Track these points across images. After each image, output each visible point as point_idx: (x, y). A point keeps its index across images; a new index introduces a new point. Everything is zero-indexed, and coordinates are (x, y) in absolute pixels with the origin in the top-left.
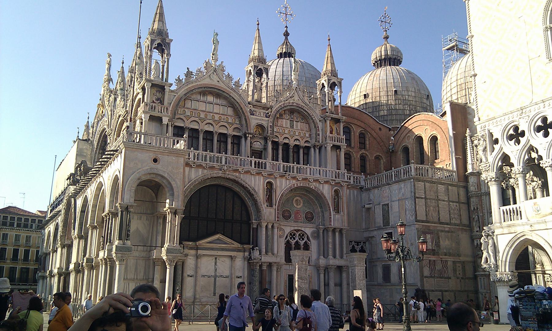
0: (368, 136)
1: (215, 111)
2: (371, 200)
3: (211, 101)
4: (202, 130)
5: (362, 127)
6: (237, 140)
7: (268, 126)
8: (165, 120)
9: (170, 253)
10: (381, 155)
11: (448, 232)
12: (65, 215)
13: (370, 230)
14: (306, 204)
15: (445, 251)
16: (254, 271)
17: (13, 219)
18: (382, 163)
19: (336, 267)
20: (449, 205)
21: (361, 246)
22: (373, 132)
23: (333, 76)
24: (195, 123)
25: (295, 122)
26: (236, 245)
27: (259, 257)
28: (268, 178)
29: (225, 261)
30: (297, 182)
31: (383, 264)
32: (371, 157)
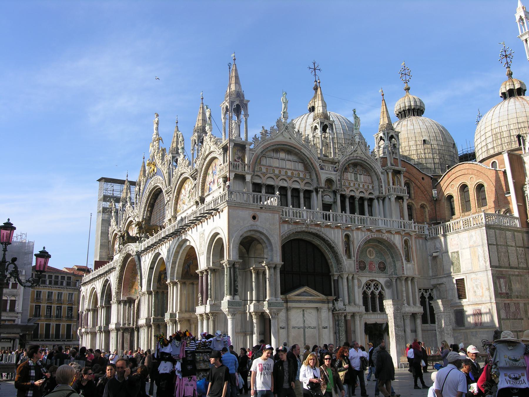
0: (412, 185)
1: (288, 167)
2: (437, 248)
4: (277, 186)
5: (407, 177)
6: (308, 194)
8: (248, 178)
10: (425, 203)
11: (518, 275)
12: (120, 272)
13: (438, 277)
14: (378, 255)
15: (517, 294)
16: (340, 322)
17: (57, 277)
18: (427, 211)
19: (411, 314)
20: (516, 250)
21: (429, 293)
23: (391, 129)
25: (358, 175)
26: (322, 297)
28: (346, 231)
29: (311, 312)
30: (371, 234)
31: (455, 309)
32: (417, 206)
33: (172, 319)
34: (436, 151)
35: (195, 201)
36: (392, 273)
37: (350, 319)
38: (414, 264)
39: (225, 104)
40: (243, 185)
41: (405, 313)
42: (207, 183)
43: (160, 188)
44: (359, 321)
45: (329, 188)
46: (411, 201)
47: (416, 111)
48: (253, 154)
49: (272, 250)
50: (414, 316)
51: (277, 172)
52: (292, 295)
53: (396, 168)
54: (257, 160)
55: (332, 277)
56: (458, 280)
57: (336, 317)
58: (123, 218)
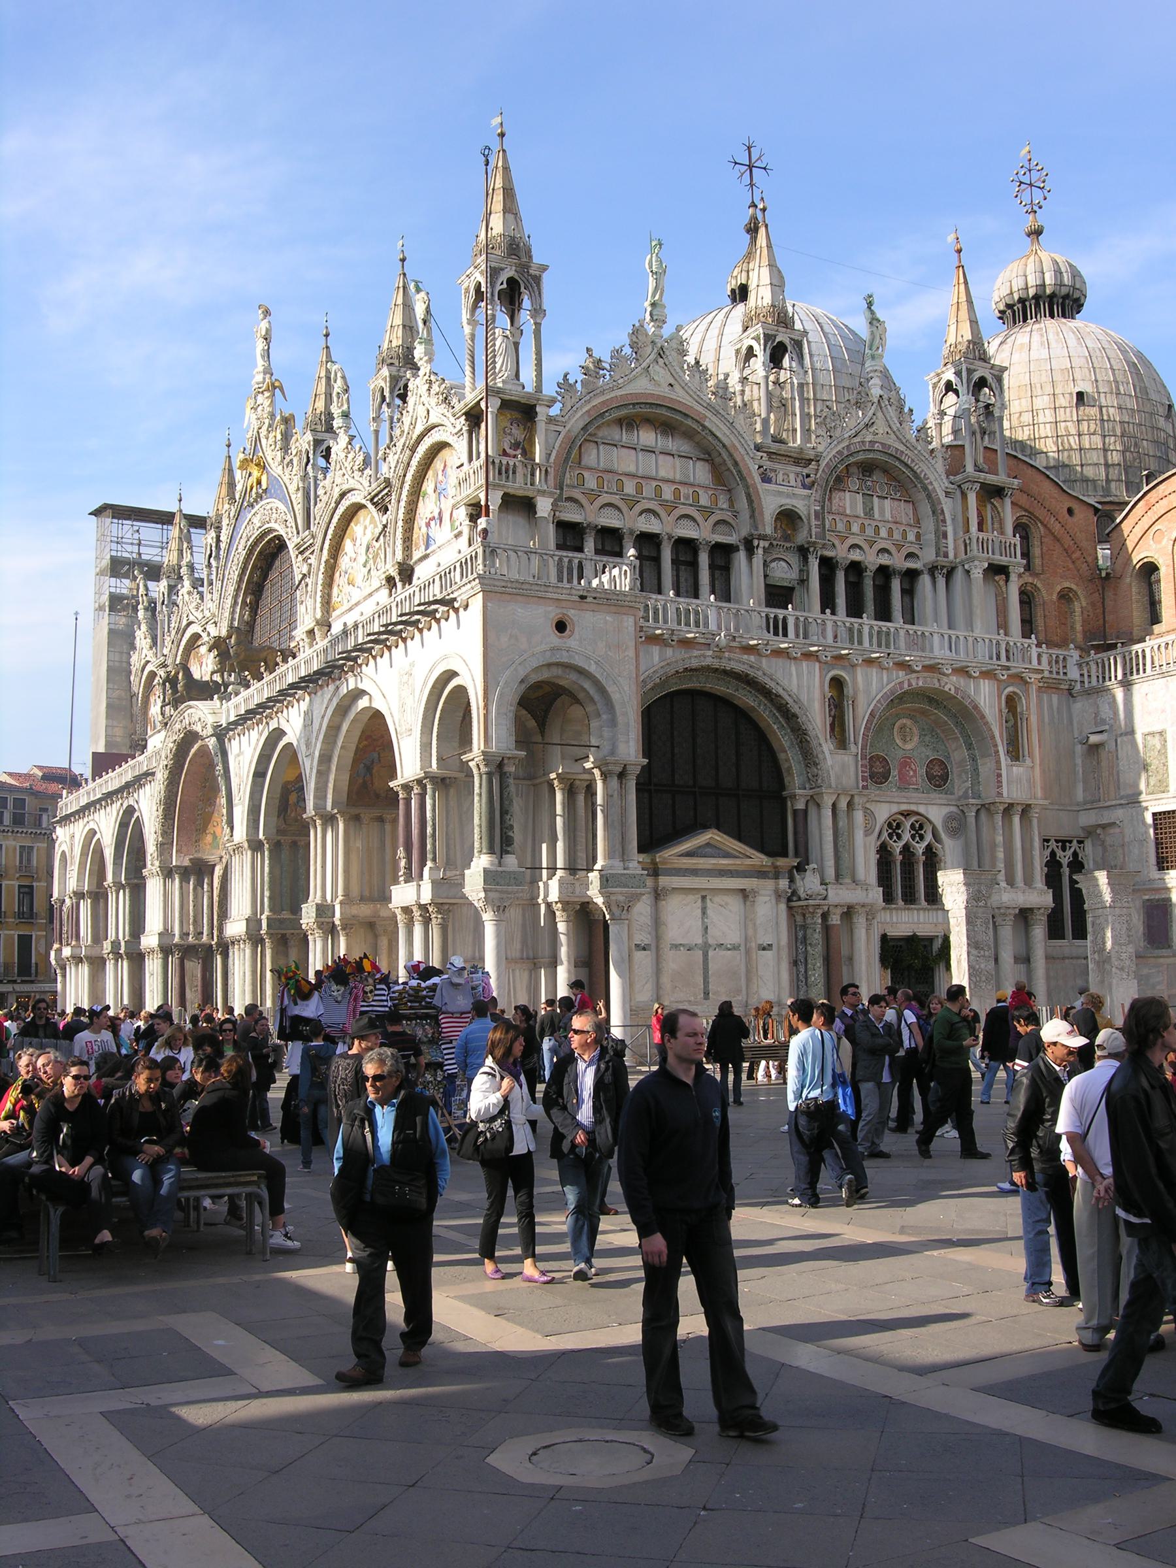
0: (1037, 532)
1: (663, 473)
2: (1103, 722)
3: (648, 444)
4: (631, 532)
5: (1021, 507)
6: (722, 554)
7: (809, 514)
8: (544, 506)
9: (620, 887)
10: (1074, 587)
12: (167, 785)
14: (927, 739)
16: (809, 931)
18: (1078, 610)
19: (1017, 911)
21: (1072, 850)
22: (1053, 519)
23: (980, 359)
24: (609, 511)
25: (876, 499)
26: (759, 859)
27: (819, 889)
28: (833, 667)
29: (727, 904)
30: (908, 677)
31: (1147, 897)
32: (1048, 595)
33: (323, 920)
34: (1114, 427)
35: (384, 576)
36: (966, 792)
37: (839, 922)
38: (1032, 767)
39: (472, 278)
40: (527, 526)
41: (999, 908)
42: (420, 522)
43: (279, 537)
44: (863, 931)
45: (787, 538)
46: (1030, 580)
47: (1060, 301)
48: (560, 433)
49: (613, 723)
50: (1024, 915)
51: (630, 488)
52: (670, 855)
53: (991, 479)
54: (569, 453)
55: (789, 804)
56: (1160, 813)
57: (799, 919)
58: (172, 625)
